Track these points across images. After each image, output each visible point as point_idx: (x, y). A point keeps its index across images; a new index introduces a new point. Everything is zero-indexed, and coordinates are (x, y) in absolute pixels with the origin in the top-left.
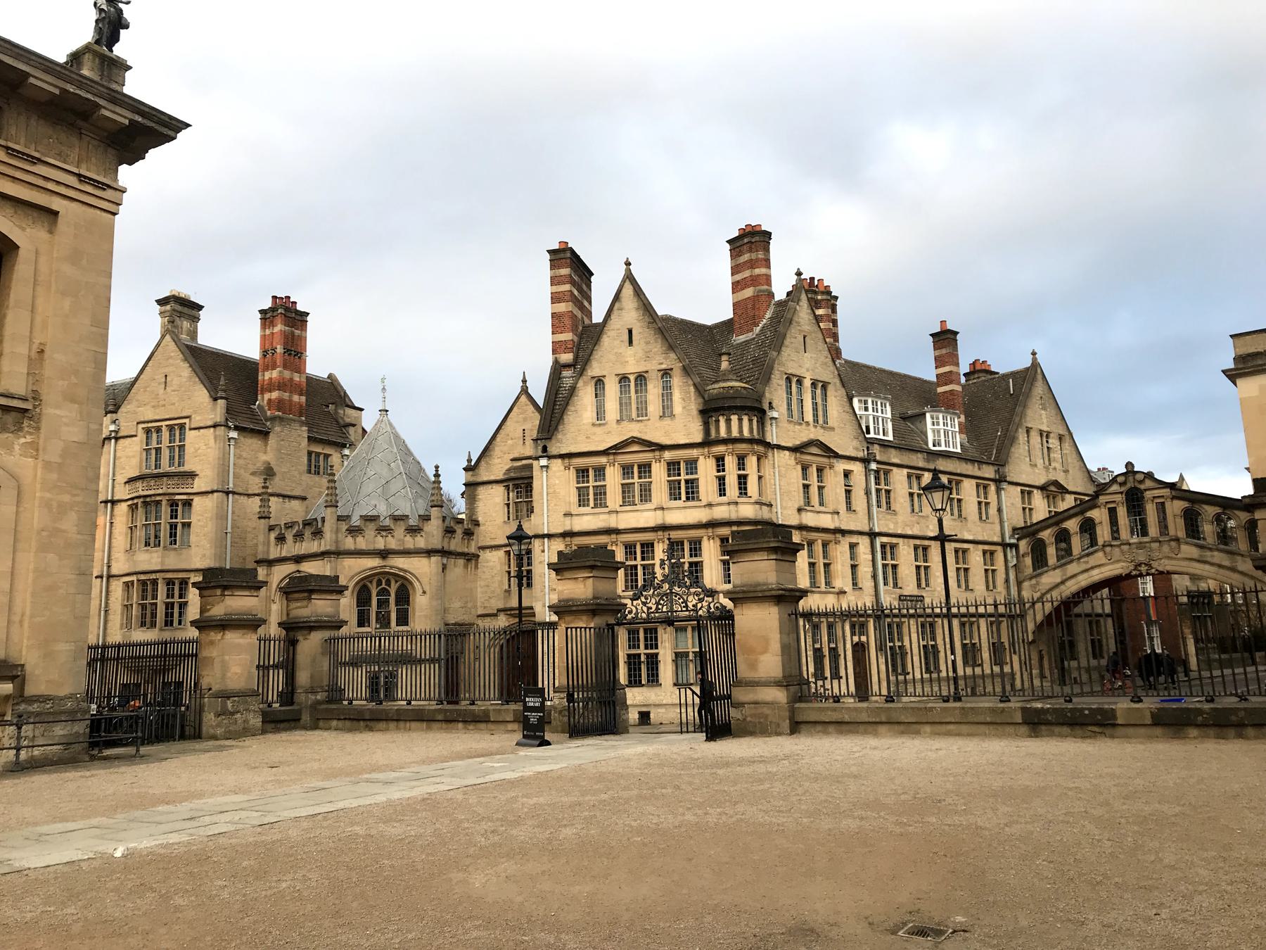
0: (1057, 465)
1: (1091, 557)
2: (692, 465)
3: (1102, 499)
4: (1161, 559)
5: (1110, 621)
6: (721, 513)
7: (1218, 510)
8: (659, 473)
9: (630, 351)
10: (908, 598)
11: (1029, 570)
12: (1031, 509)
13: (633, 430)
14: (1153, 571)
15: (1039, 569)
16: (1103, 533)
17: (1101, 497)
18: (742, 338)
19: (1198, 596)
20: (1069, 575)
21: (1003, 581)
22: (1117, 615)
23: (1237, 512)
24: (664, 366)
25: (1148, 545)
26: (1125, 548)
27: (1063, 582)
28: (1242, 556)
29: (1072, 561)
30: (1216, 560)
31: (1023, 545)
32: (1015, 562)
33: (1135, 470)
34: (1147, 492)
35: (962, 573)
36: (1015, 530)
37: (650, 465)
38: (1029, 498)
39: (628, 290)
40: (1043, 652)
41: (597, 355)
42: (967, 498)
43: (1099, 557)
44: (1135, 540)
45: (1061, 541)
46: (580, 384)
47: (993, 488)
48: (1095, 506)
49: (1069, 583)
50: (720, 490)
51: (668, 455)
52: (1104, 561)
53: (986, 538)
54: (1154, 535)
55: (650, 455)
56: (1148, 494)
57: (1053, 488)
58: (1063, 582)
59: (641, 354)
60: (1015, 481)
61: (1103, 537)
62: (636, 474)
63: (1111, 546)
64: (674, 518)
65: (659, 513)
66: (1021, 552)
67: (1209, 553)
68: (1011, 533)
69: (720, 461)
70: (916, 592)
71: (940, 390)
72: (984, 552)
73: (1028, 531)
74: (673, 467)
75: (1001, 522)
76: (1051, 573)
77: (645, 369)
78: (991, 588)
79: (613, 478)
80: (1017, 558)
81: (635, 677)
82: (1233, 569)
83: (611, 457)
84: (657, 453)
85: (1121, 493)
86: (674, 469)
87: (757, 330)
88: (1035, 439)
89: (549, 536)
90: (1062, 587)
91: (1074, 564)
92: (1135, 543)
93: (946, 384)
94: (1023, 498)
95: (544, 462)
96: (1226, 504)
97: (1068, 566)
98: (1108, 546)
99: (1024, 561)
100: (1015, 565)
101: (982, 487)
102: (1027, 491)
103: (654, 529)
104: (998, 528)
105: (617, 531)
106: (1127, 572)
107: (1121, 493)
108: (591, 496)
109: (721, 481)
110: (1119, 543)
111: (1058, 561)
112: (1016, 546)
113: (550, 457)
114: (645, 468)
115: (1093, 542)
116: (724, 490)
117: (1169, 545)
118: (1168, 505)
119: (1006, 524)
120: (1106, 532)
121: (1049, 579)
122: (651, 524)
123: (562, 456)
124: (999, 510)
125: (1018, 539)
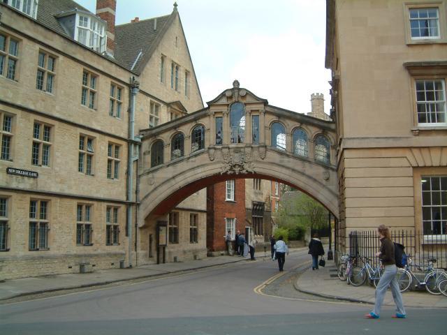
0: (182, 90)
1: (198, 157)
3: (213, 109)
4: (251, 162)
5: (205, 215)
7: (298, 125)
10: (19, 172)
11: (148, 167)
12: (157, 120)
14: (244, 171)
15: (155, 165)
16: (210, 139)
19: (257, 205)
21: (125, 172)
22: (210, 212)
25: (242, 150)
26: (226, 151)
27: (174, 178)
28: (310, 162)
29: (182, 160)
30: (290, 165)
31: (147, 146)
34: (247, 106)
35: (85, 158)
36: (141, 131)
38: (157, 110)
40: (153, 236)
42: (101, 92)
43: (204, 158)
44: (233, 145)
45: (176, 148)
47: (126, 91)
48: (205, 116)
49: (178, 179)
52: (208, 161)
53: (113, 132)
54: (248, 142)
57: (176, 108)
58: (174, 178)
60: (147, 91)
61: (210, 141)
63: (215, 149)
67: (286, 159)
68: (137, 134)
70: (31, 167)
72: (110, 145)
73: (152, 134)
75: (130, 123)
78: (113, 176)
80: (140, 154)
82: (303, 174)
88: (168, 66)
90: (173, 182)
91: (184, 163)
93: (104, 7)
94: (152, 108)
101: (117, 85)
102: (155, 105)
104: (126, 126)
107: (228, 105)
110: (220, 147)
111: (172, 160)
112: (140, 146)
115: (201, 145)
117: (259, 151)
118: (261, 117)
119: (134, 124)
120: (212, 137)
121: (163, 174)
124: (130, 111)
125: (142, 139)
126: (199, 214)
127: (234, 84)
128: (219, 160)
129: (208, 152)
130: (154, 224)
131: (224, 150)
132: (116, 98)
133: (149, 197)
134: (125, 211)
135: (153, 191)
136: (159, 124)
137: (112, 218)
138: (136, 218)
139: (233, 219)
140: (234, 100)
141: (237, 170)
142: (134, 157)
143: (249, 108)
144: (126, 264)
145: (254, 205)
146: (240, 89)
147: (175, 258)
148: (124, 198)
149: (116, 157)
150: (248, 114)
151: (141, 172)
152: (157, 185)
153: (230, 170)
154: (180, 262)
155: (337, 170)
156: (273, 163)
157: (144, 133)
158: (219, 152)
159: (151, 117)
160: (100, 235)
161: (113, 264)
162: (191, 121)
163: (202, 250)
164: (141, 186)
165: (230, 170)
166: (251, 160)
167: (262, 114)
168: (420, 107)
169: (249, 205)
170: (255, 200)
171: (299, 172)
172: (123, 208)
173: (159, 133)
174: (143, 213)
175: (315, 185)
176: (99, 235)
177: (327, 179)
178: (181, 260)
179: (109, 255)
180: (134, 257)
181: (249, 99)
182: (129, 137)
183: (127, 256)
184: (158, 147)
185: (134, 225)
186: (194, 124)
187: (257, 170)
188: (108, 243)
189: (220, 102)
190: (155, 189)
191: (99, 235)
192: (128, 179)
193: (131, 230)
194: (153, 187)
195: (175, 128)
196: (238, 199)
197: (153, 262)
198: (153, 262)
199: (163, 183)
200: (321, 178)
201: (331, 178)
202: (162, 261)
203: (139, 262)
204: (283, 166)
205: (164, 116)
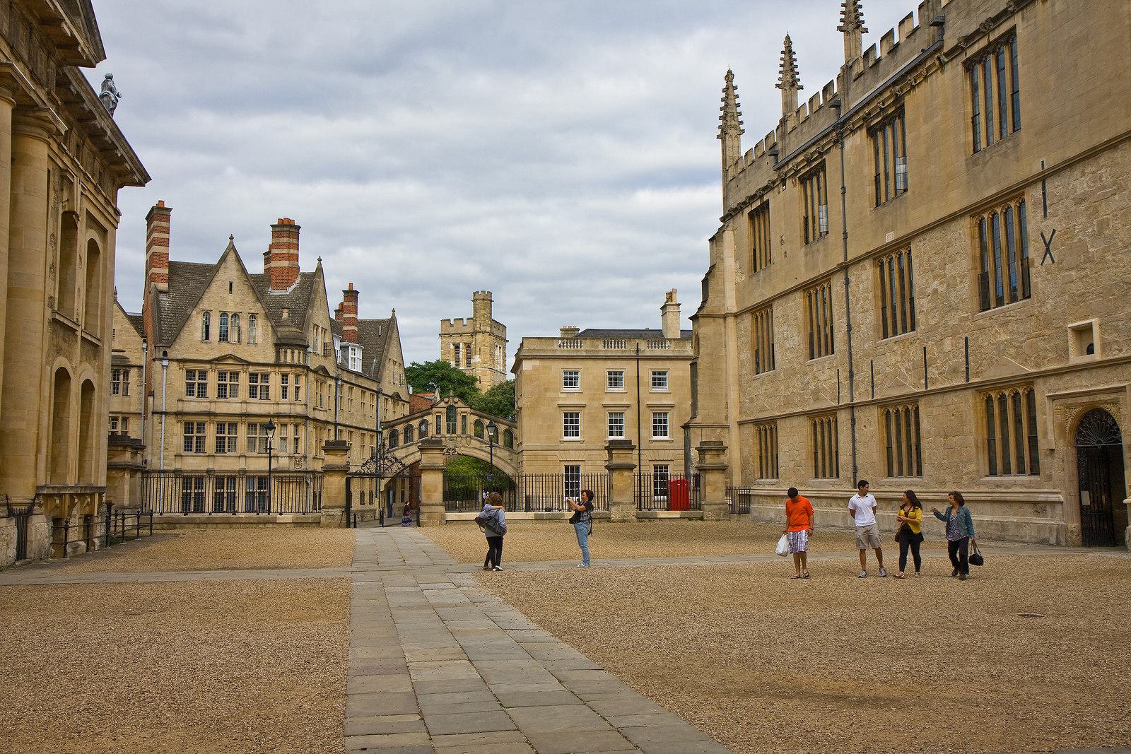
2: (265, 377)
3: (434, 410)
6: (284, 409)
8: (244, 380)
9: (230, 297)
13: (226, 349)
18: (277, 293)
24: (253, 311)
27: (406, 457)
29: (413, 444)
31: (386, 433)
37: (238, 374)
39: (232, 257)
41: (207, 295)
46: (194, 313)
47: (376, 397)
48: (429, 414)
49: (409, 457)
50: (283, 395)
51: (252, 369)
55: (240, 367)
56: (459, 410)
58: (406, 457)
59: (238, 300)
62: (228, 379)
64: (254, 409)
65: (244, 405)
69: (285, 377)
71: (345, 328)
73: (390, 425)
74: (253, 377)
75: (377, 418)
76: (399, 451)
77: (241, 311)
79: (212, 380)
81: (219, 505)
83: (214, 365)
84: (245, 367)
86: (253, 378)
87: (291, 289)
89: (166, 413)
95: (165, 363)
103: (241, 415)
105: (215, 415)
108: (196, 387)
109: (285, 389)
113: (170, 360)
114: (235, 375)
116: (286, 395)
122: (238, 412)
123: (179, 361)
124: (377, 411)
125: (383, 429)
168: (566, 428)
173: (396, 425)
174: (384, 482)
176: (367, 498)
184: (394, 436)
186: (420, 419)
187: (464, 452)
191: (367, 498)
195: (407, 421)
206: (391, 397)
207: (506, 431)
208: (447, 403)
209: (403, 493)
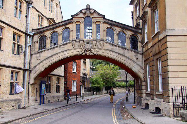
0: (55, 14)
1: (66, 45)
4: (95, 49)
5: (63, 78)
7: (121, 30)
11: (37, 50)
12: (41, 26)
14: (92, 54)
16: (73, 35)
17: (74, 19)
20: (55, 53)
22: (66, 77)
23: (128, 31)
25: (91, 42)
26: (82, 42)
27: (52, 56)
28: (127, 50)
29: (57, 47)
30: (117, 51)
31: (36, 38)
32: (31, 44)
33: (90, 8)
34: (94, 19)
36: (33, 30)
38: (42, 21)
43: (69, 46)
49: (54, 57)
52: (72, 48)
58: (52, 56)
61: (73, 36)
63: (76, 41)
66: (34, 40)
67: (115, 48)
72: (14, 34)
73: (40, 32)
76: (47, 52)
80: (32, 43)
82: (124, 56)
85: (83, 18)
90: (51, 58)
91: (58, 48)
92: (85, 41)
94: (39, 19)
96: (124, 27)
97: (55, 49)
98: (74, 40)
99: (35, 45)
100: (30, 46)
102: (41, 16)
106: (81, 53)
107: (83, 18)
111: (51, 46)
112: (32, 38)
121: (46, 54)
124: (26, 16)
125: (34, 34)
126: (61, 78)
127: (87, 6)
128: (78, 47)
129: (72, 43)
130: (38, 82)
131: (80, 42)
132: (18, 7)
133: (37, 67)
134: (23, 73)
135: (39, 63)
136: (43, 27)
137: (14, 78)
138: (29, 78)
139: (75, 81)
140: (86, 15)
141: (88, 53)
142: (29, 44)
143: (95, 20)
144: (22, 106)
145: (83, 75)
146: (90, 9)
147: (49, 101)
148: (22, 67)
149: (18, 42)
150: (94, 23)
151: (33, 52)
152: (43, 60)
153: (84, 53)
154: (51, 103)
155: (143, 53)
156: (107, 50)
157: (35, 31)
158: (78, 43)
159: (39, 24)
160: (6, 89)
161: (13, 106)
162: (62, 26)
163: (62, 96)
164: (32, 60)
165: (84, 53)
166: (94, 48)
167: (102, 23)
169: (81, 75)
170: (84, 72)
171: (122, 55)
172: (21, 72)
174: (33, 75)
175: (130, 62)
177: (137, 59)
178: (52, 102)
179: (12, 100)
180: (27, 101)
181: (95, 15)
182: (26, 31)
183: (23, 101)
185: (28, 83)
186: (64, 27)
187: (99, 53)
188: (11, 93)
189: (79, 16)
190: (41, 62)
192: (25, 56)
193: (26, 85)
194: (39, 61)
195: (53, 29)
196: (77, 71)
197: (38, 104)
198: (38, 104)
199: (46, 59)
200: (133, 58)
201: (139, 58)
202: (42, 103)
203: (30, 104)
204: (113, 51)
205: (45, 23)
206: (48, 19)
207: (132, 36)
208: (84, 14)
209: (58, 88)
